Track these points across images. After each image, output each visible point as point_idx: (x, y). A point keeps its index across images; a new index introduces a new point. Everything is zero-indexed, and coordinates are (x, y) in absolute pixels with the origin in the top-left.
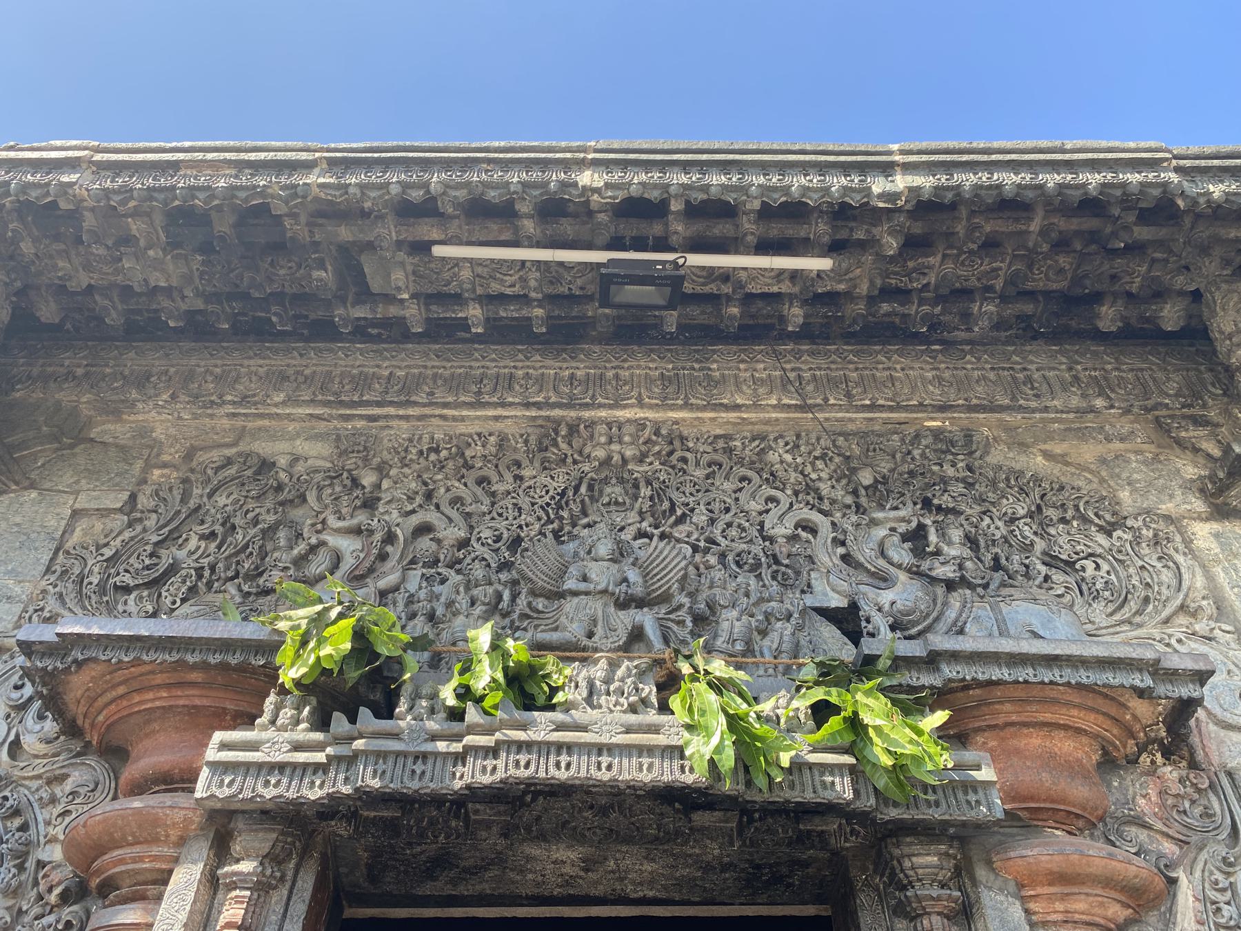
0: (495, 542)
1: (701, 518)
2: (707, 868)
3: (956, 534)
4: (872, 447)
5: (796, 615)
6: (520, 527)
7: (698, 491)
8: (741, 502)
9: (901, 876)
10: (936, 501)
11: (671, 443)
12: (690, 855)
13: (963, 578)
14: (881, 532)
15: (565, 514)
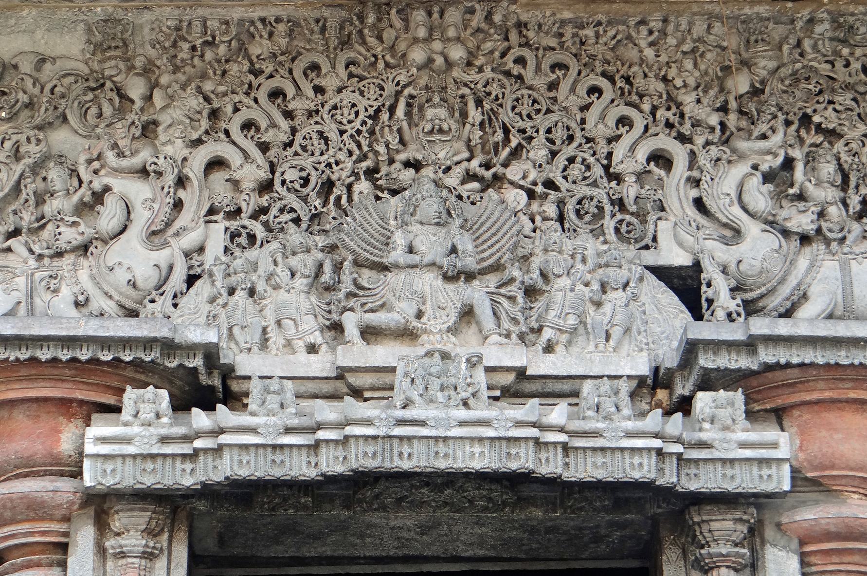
0: (302, 186)
1: (539, 153)
2: (533, 531)
3: (828, 169)
4: (753, 38)
5: (631, 284)
6: (329, 165)
7: (538, 111)
8: (588, 126)
9: (700, 537)
10: (816, 119)
11: (507, 39)
12: (517, 521)
13: (819, 231)
14: (742, 169)
15: (381, 149)
